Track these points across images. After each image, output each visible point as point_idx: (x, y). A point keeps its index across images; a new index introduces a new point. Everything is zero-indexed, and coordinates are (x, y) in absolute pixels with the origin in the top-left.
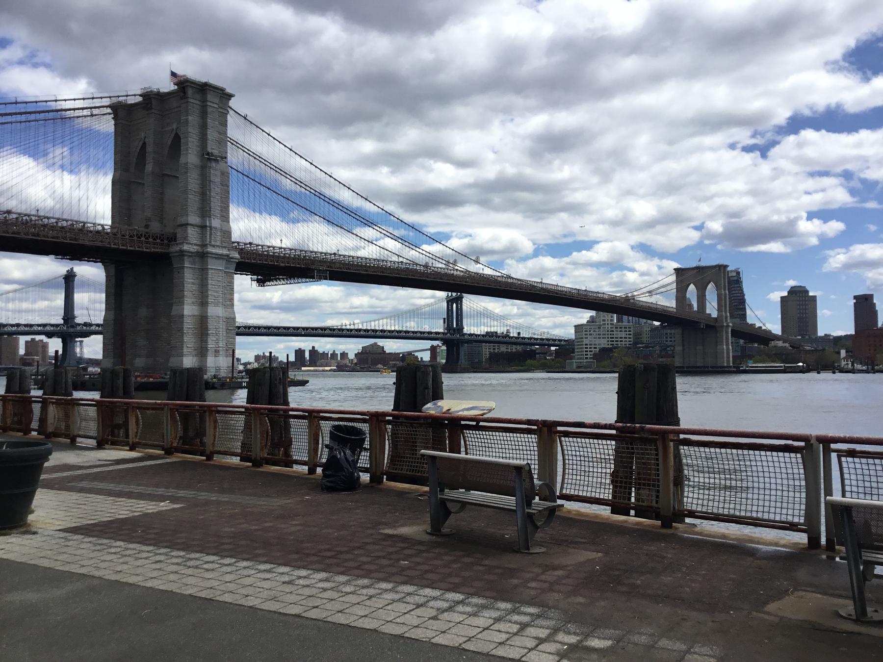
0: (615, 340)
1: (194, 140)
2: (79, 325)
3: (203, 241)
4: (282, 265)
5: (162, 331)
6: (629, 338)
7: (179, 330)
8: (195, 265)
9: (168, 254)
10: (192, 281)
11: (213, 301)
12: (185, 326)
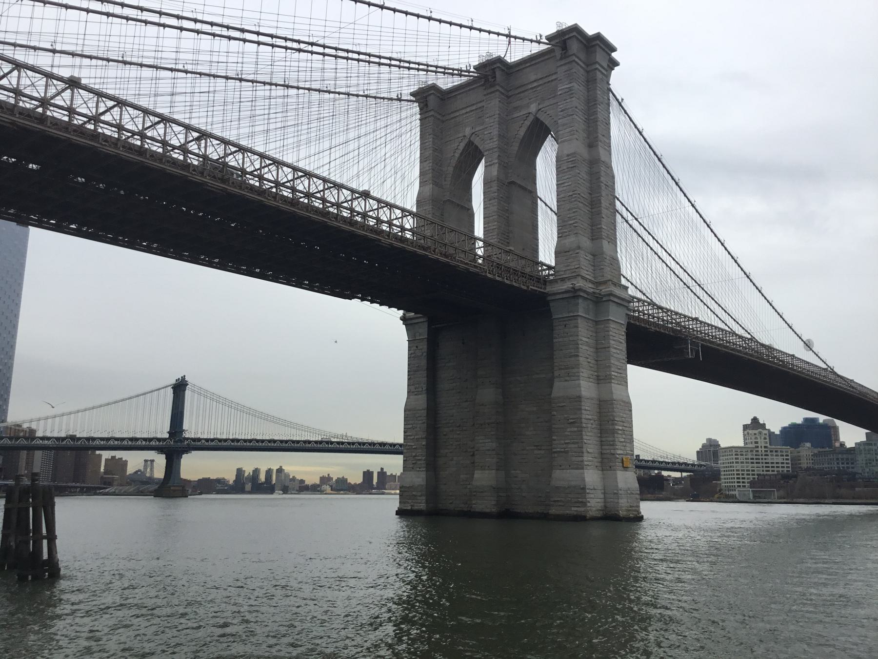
0: (770, 465)
1: (581, 120)
2: (187, 439)
3: (595, 278)
6: (786, 463)
7: (572, 423)
9: (547, 294)
10: (587, 340)
11: (616, 374)
12: (584, 416)
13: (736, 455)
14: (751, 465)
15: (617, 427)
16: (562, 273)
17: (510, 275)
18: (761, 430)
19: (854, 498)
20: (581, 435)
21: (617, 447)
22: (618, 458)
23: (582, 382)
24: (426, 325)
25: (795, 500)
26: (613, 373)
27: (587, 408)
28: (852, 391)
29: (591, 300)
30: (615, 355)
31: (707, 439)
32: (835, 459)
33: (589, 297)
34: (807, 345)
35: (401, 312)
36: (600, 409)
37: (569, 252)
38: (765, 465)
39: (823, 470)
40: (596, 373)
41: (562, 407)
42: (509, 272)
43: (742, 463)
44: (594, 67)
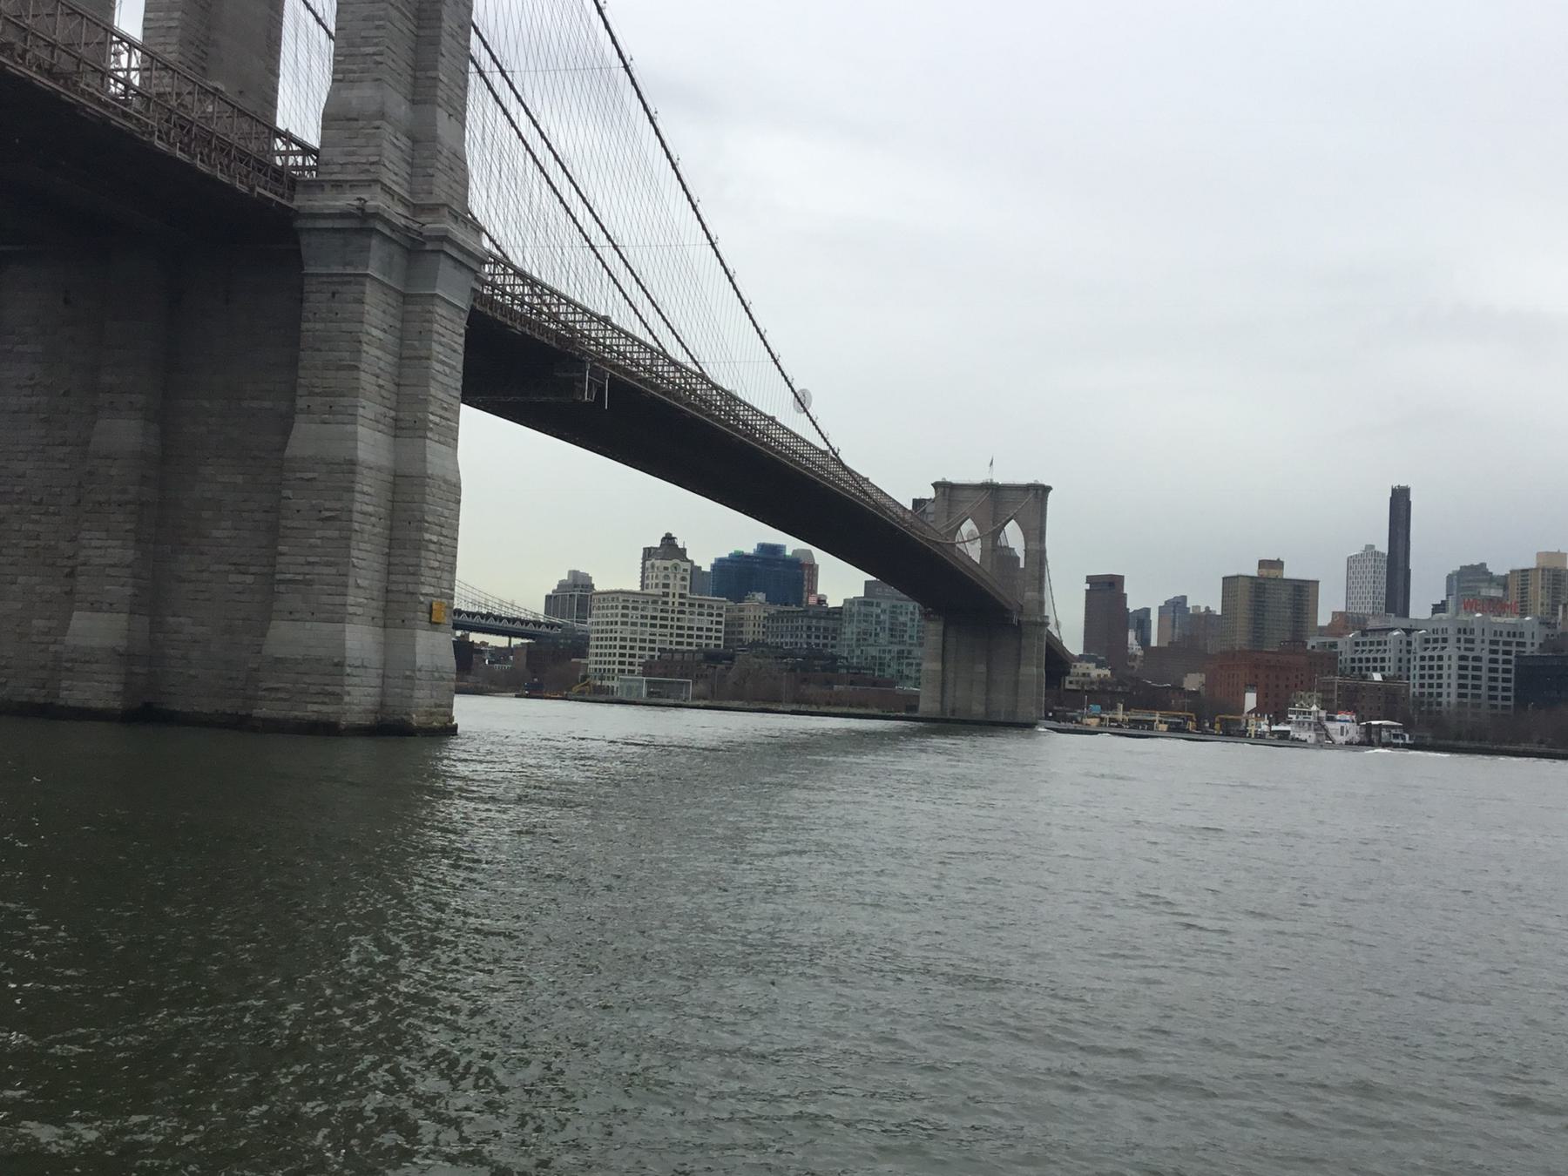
0: (686, 632)
3: (411, 193)
5: (206, 514)
6: (717, 631)
8: (390, 278)
9: (297, 214)
11: (437, 420)
12: (357, 506)
13: (623, 608)
14: (649, 629)
15: (427, 536)
16: (337, 168)
17: (211, 151)
18: (677, 561)
19: (828, 704)
20: (348, 547)
21: (423, 579)
22: (422, 603)
23: (360, 429)
25: (725, 704)
26: (431, 417)
27: (366, 489)
28: (863, 500)
29: (400, 245)
30: (440, 377)
31: (570, 572)
32: (805, 629)
33: (394, 236)
34: (799, 400)
36: (394, 493)
37: (356, 120)
38: (675, 631)
39: (781, 647)
40: (393, 413)
41: (308, 480)
42: (209, 143)
43: (634, 624)
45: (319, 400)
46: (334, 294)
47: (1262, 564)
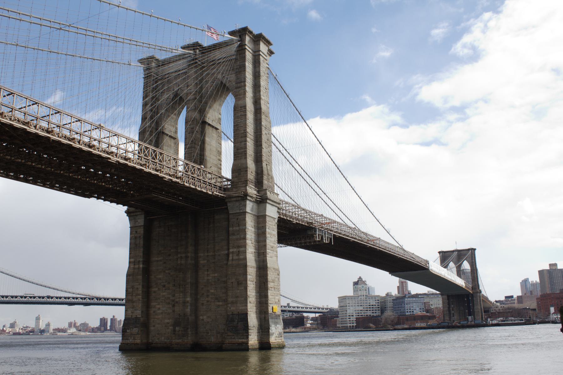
4: (295, 221)
24: (143, 216)
35: (126, 208)
38: (365, 307)
44: (257, 54)
45: (235, 250)
46: (237, 219)
47: (550, 265)
